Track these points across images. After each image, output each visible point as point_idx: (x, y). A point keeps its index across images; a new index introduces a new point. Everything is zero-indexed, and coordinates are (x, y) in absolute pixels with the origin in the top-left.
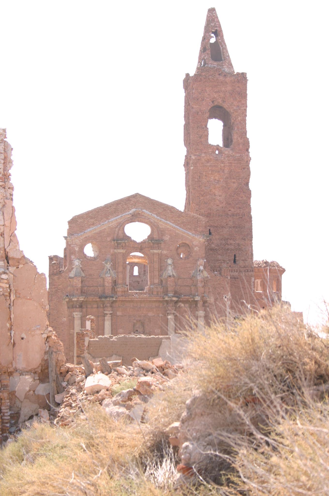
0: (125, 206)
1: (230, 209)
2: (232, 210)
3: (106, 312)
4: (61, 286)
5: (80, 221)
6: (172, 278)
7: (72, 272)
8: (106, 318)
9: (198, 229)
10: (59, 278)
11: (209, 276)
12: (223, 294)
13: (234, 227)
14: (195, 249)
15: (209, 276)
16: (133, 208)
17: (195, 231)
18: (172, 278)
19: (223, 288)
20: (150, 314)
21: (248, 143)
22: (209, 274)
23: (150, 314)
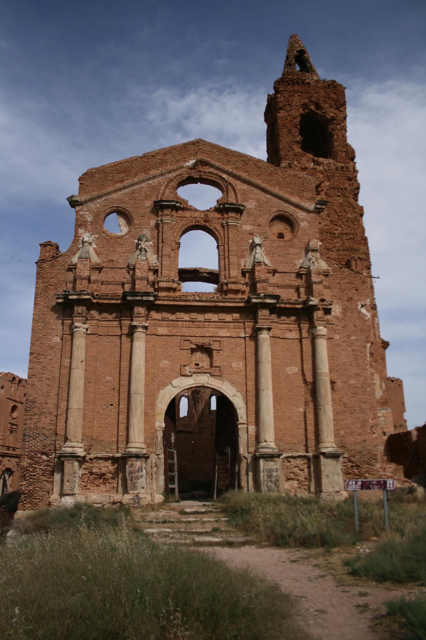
0: (179, 157)
1: (337, 228)
2: (340, 229)
3: (134, 323)
4: (54, 281)
5: (98, 176)
6: (263, 267)
7: (77, 255)
8: (136, 335)
9: (305, 194)
10: (52, 266)
11: (329, 268)
12: (357, 301)
13: (343, 250)
14: (302, 224)
15: (329, 268)
16: (192, 160)
17: (299, 196)
18: (263, 267)
19: (356, 290)
20: (223, 333)
21: (353, 151)
22: (329, 266)
23: (223, 333)
